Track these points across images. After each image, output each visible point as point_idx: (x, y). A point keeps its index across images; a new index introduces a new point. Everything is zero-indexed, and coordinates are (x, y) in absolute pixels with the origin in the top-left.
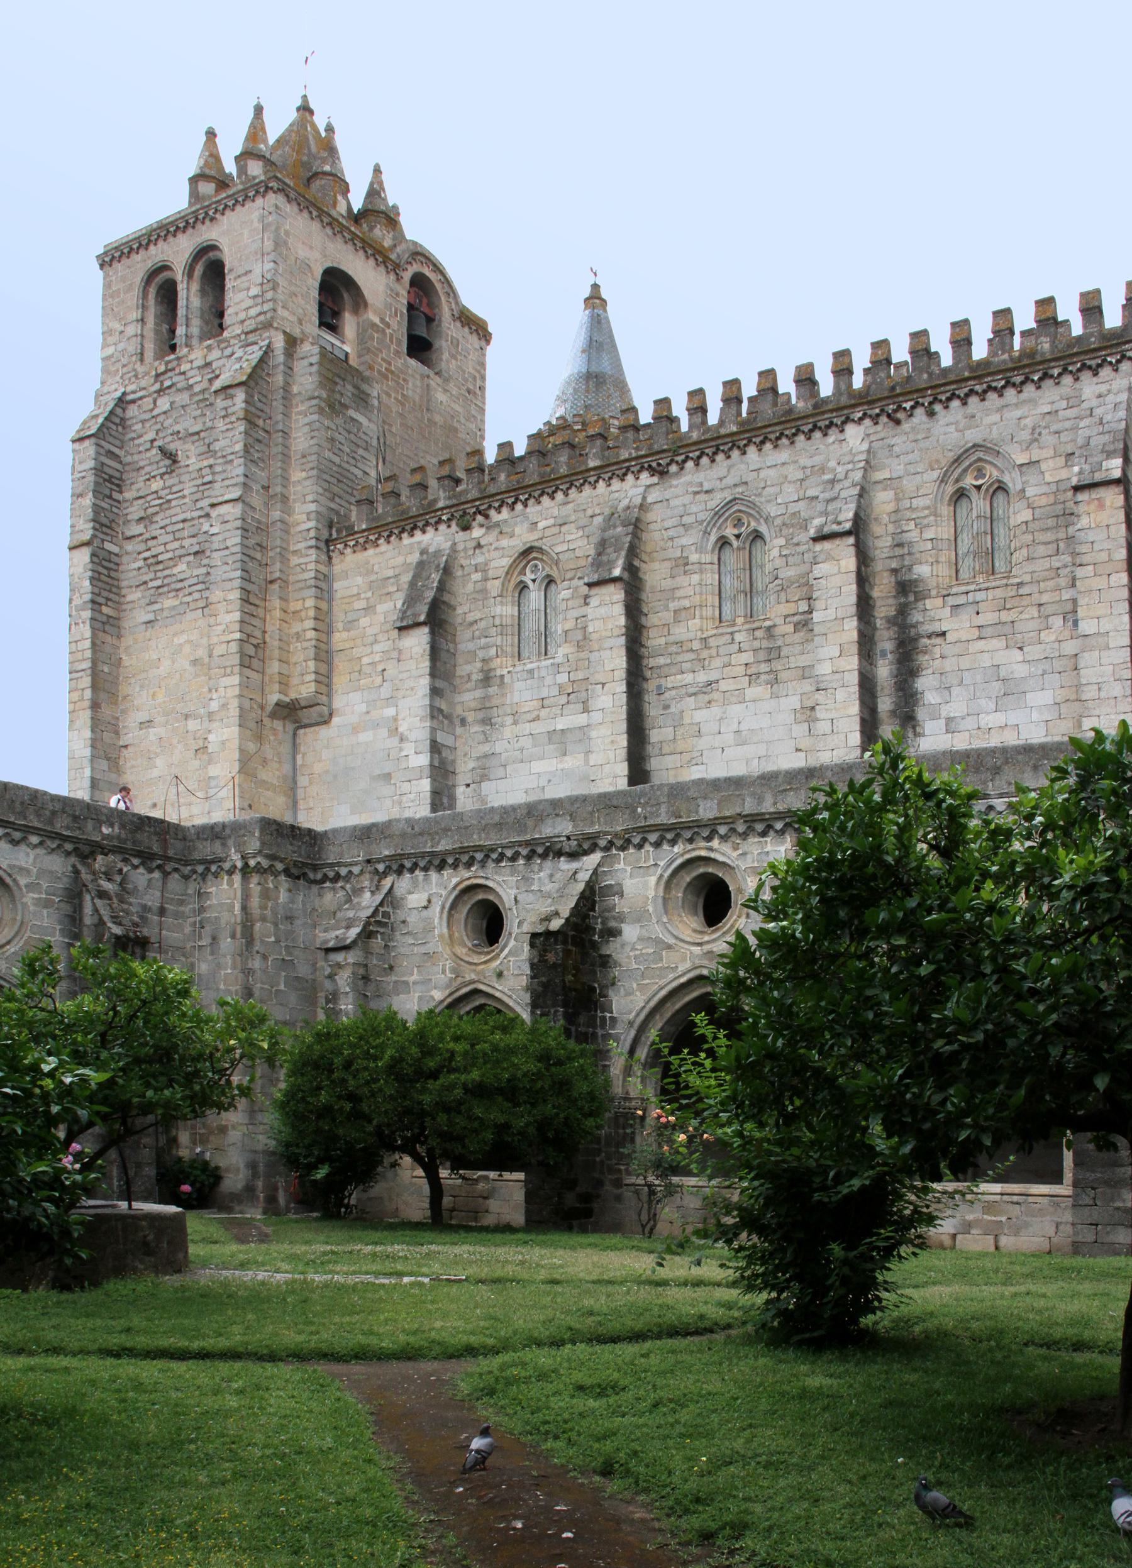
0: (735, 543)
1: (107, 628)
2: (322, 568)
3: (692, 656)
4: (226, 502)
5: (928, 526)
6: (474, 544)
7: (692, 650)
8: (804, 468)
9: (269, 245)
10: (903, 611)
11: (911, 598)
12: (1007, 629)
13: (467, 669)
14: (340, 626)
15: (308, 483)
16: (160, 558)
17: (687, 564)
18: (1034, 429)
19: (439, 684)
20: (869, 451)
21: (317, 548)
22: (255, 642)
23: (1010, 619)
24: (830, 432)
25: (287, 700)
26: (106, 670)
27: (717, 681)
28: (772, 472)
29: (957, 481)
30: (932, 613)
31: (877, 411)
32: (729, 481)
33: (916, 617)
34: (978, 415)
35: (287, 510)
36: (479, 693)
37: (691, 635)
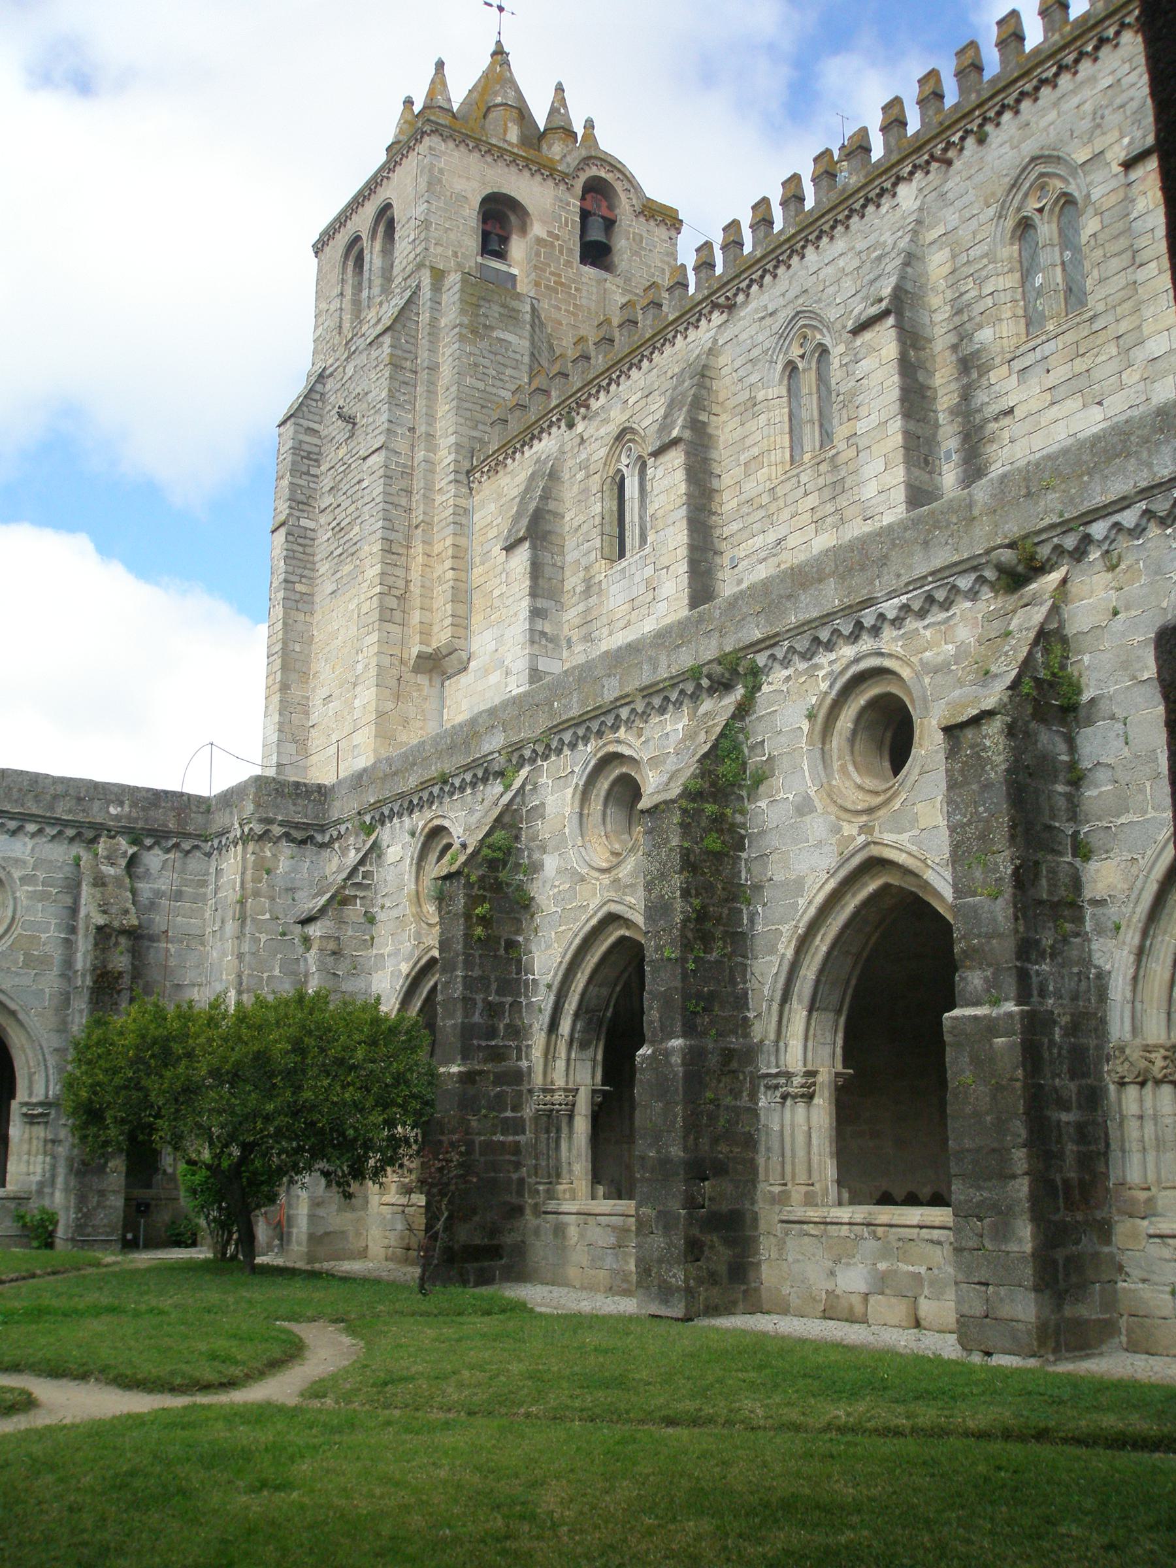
0: (800, 366)
1: (300, 606)
2: (462, 502)
3: (761, 513)
4: (373, 452)
5: (987, 278)
6: (578, 440)
7: (761, 506)
8: (860, 252)
9: (423, 186)
10: (966, 395)
11: (975, 375)
12: (1082, 382)
13: (573, 581)
14: (477, 560)
15: (450, 415)
16: (342, 525)
17: (755, 405)
18: (1095, 114)
19: (541, 603)
20: (921, 209)
21: (457, 481)
22: (398, 593)
23: (1085, 367)
24: (883, 200)
25: (430, 650)
26: (298, 649)
27: (784, 539)
28: (829, 270)
29: (1019, 209)
30: (997, 388)
31: (926, 157)
32: (790, 295)
33: (981, 397)
34: (1034, 120)
35: (432, 448)
36: (581, 608)
37: (761, 488)
